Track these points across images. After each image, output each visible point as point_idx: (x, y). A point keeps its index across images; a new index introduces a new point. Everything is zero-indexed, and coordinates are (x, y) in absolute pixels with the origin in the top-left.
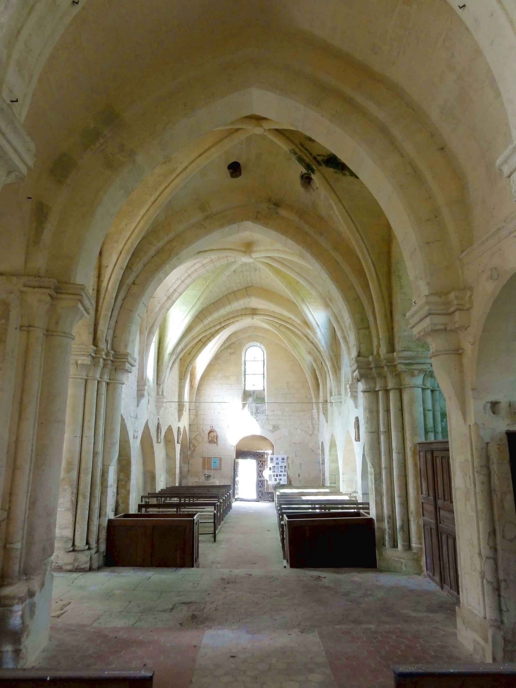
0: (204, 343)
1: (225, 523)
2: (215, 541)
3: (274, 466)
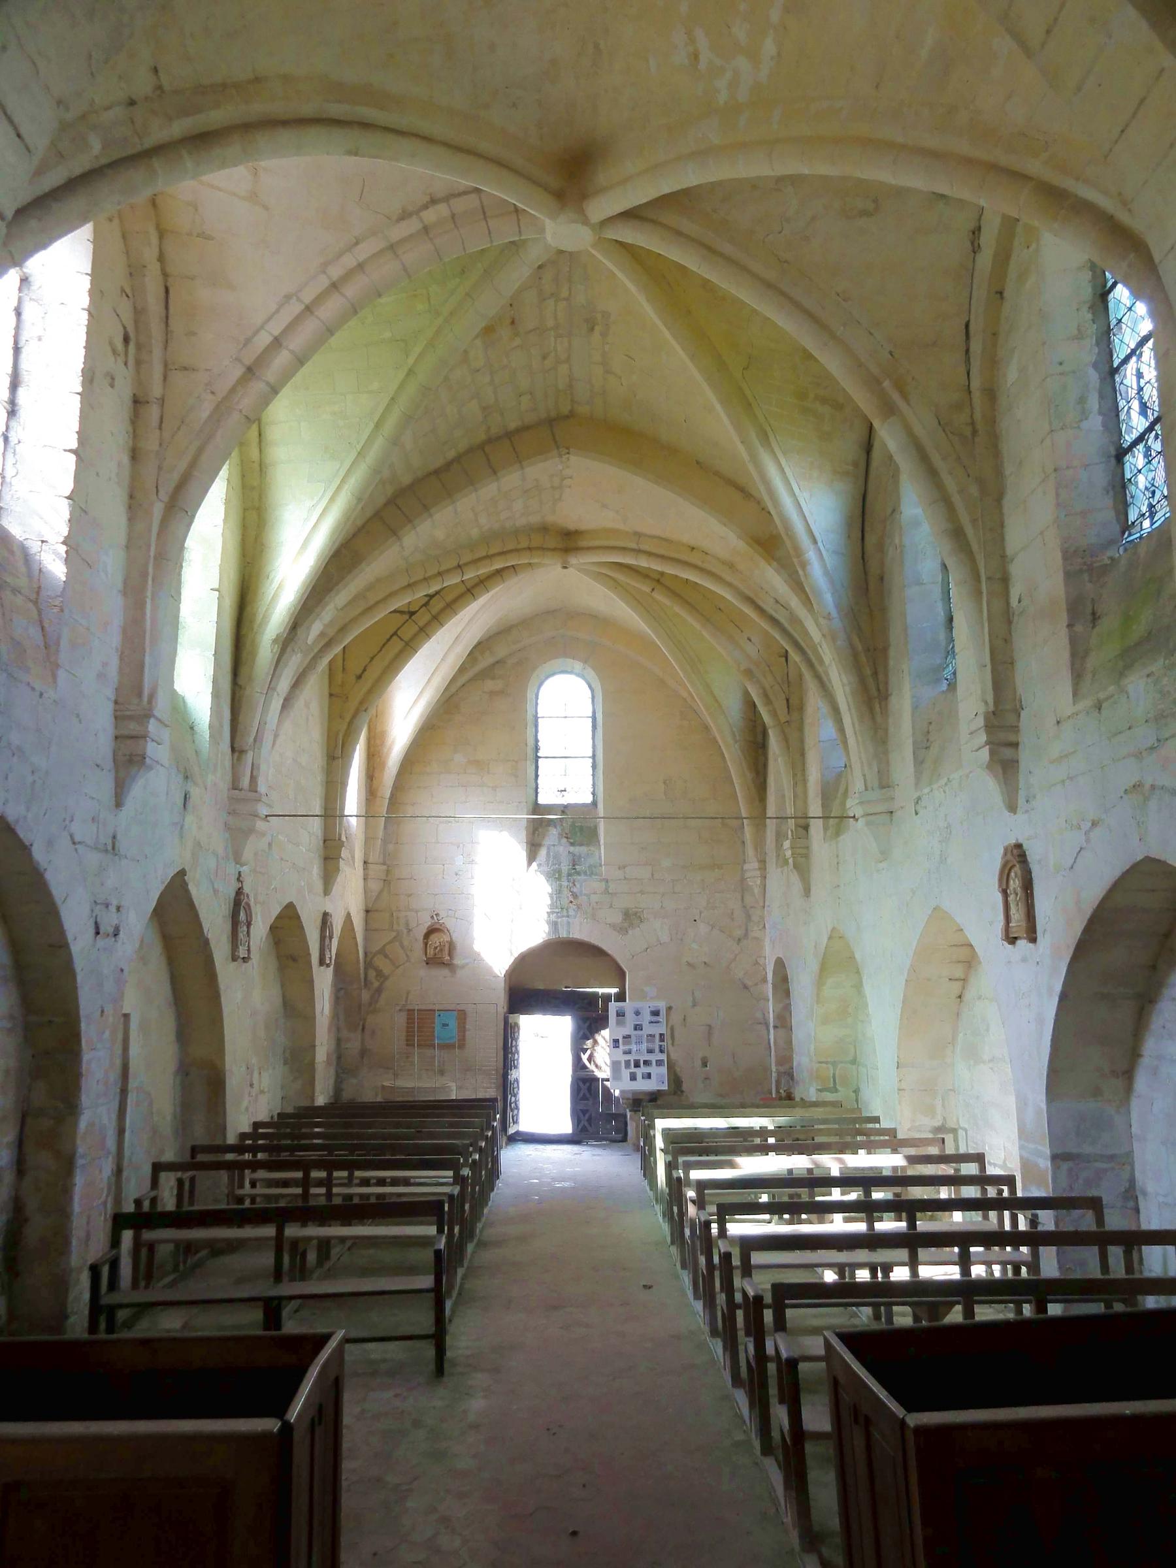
0: (407, 644)
1: (478, 1245)
2: (440, 1369)
3: (628, 1033)
